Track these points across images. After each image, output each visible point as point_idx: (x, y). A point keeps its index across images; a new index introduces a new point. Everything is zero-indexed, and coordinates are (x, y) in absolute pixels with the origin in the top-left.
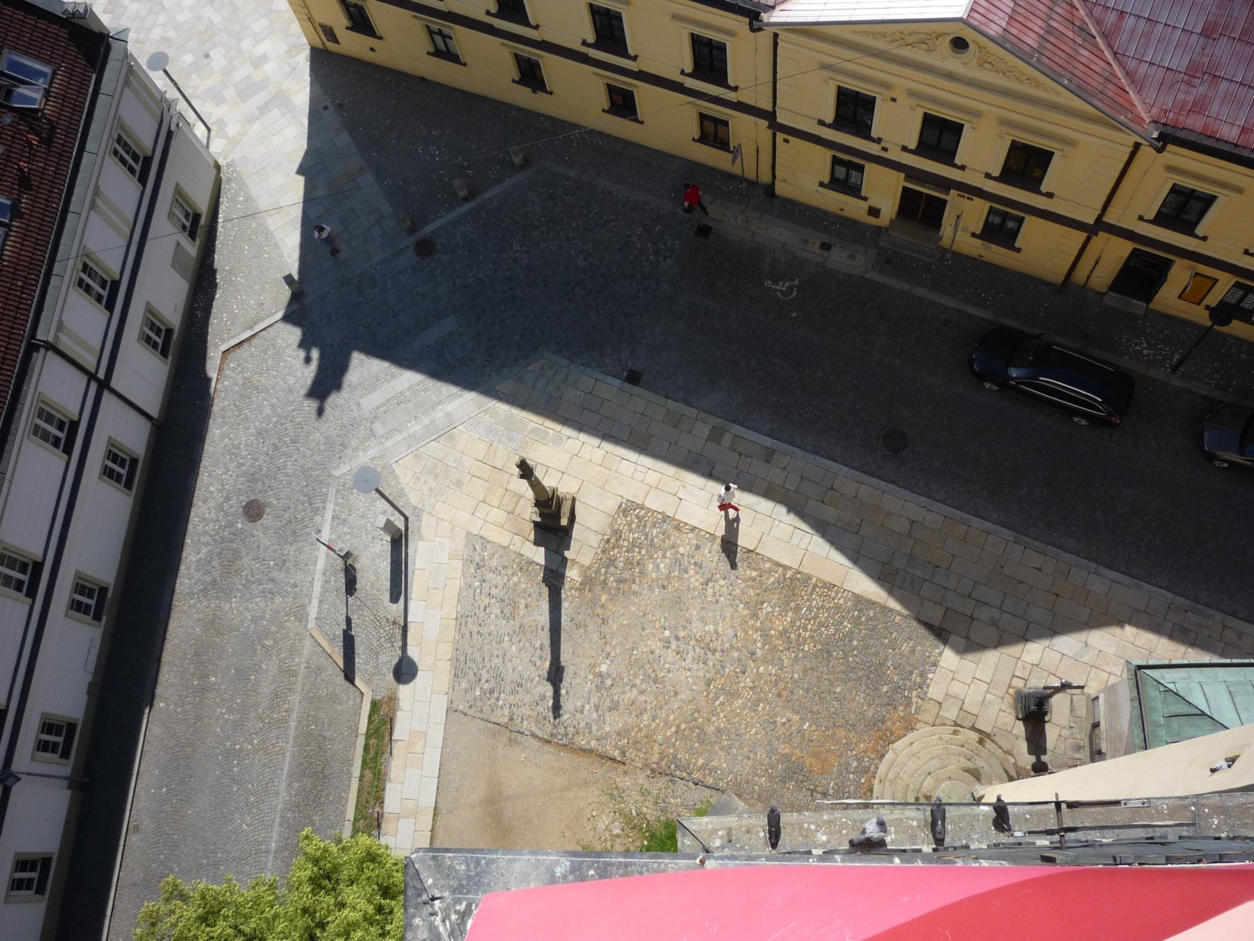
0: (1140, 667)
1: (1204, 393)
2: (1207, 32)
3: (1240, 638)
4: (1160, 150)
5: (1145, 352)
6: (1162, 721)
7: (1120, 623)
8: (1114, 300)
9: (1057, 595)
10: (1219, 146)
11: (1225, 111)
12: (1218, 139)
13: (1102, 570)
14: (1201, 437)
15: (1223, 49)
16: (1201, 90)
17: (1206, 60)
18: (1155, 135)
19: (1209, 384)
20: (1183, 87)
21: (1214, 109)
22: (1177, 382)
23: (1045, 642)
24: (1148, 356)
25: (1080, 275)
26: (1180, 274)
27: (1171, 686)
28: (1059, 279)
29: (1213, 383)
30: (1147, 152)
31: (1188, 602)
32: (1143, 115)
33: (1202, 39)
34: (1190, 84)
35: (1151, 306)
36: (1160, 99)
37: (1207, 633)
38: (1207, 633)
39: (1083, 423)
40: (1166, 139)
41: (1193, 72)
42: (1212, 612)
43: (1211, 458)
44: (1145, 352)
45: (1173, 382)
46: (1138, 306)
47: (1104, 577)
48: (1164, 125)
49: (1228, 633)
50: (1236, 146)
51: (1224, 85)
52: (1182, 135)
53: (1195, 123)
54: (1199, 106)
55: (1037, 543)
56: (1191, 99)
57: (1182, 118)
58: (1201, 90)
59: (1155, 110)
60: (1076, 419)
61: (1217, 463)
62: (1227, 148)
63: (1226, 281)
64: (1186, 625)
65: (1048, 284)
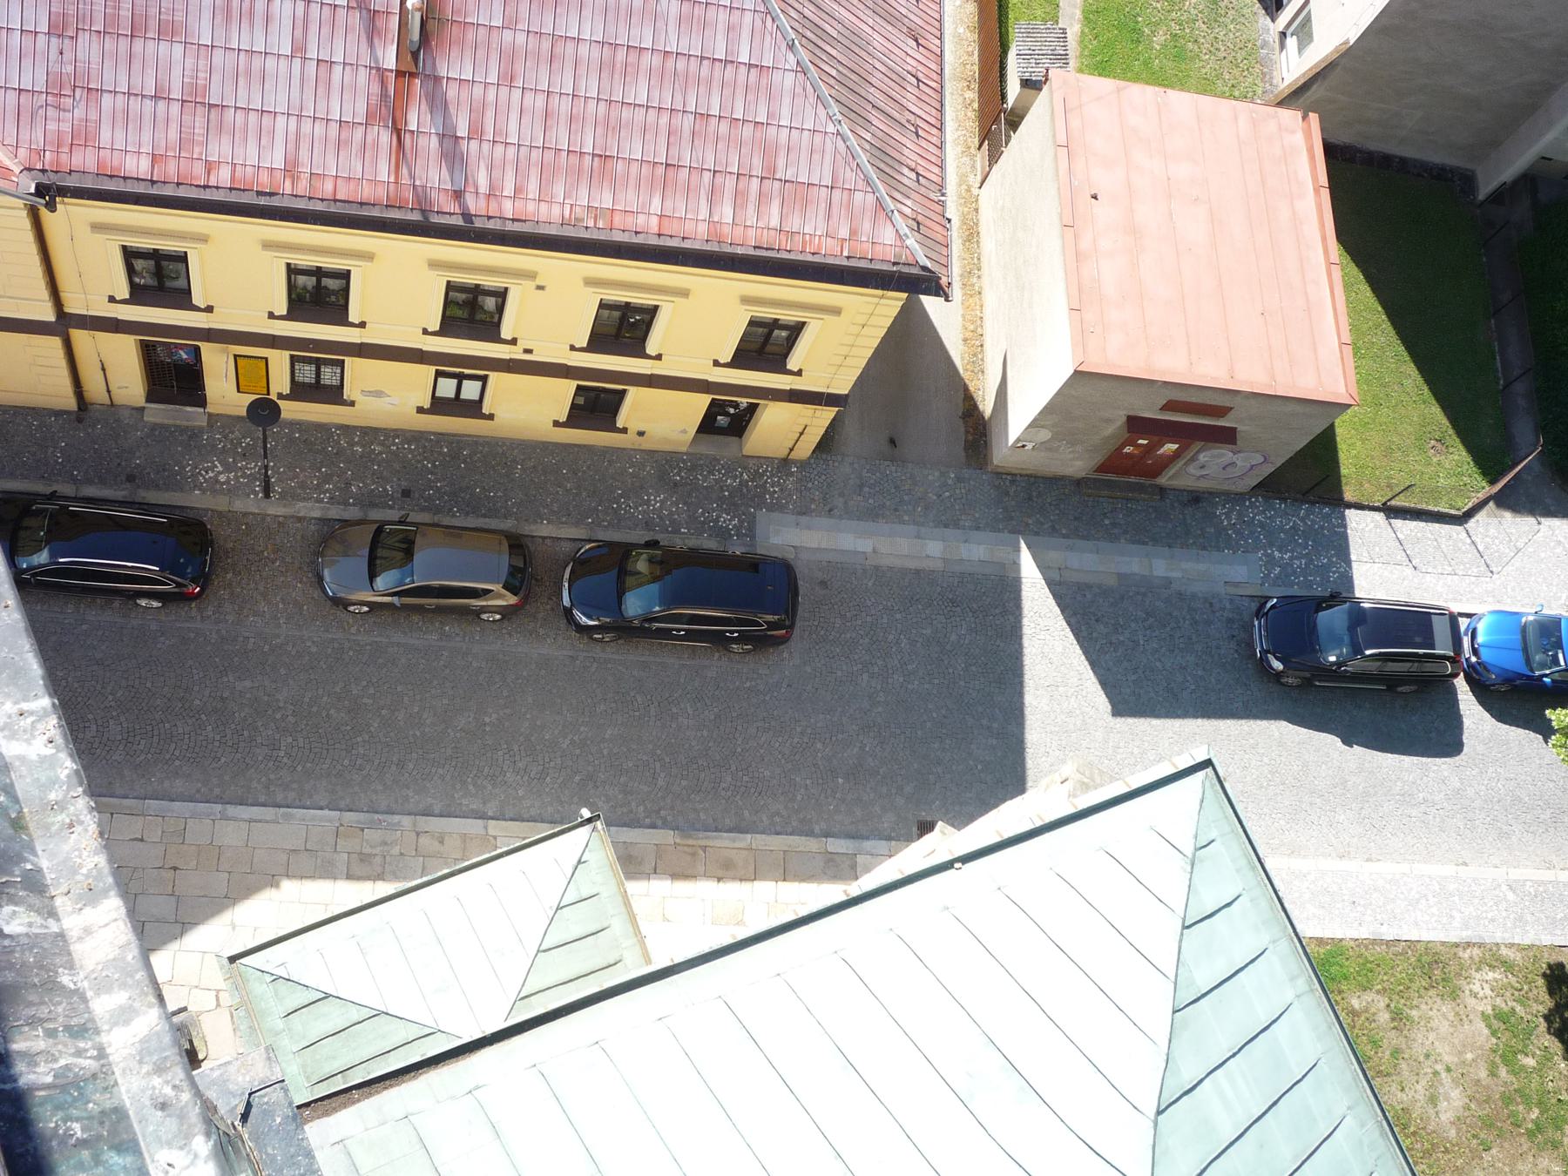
0: (232, 959)
1: (317, 514)
2: (57, 29)
3: (442, 842)
4: (51, 207)
5: (222, 478)
6: (280, 1024)
7: (273, 882)
8: (158, 413)
9: (175, 869)
10: (130, 188)
11: (120, 135)
12: (125, 178)
13: (232, 810)
14: (320, 579)
15: (88, 48)
16: (79, 113)
17: (69, 69)
18: (32, 190)
19: (321, 501)
20: (51, 112)
21: (106, 135)
22: (275, 509)
23: (174, 946)
24: (228, 482)
25: (94, 388)
26: (217, 364)
27: (281, 972)
28: (71, 403)
29: (326, 497)
30: (44, 212)
31: (362, 816)
32: (8, 163)
33: (54, 40)
34: (58, 107)
35: (210, 409)
36: (24, 135)
37: (396, 850)
38: (396, 850)
39: (155, 604)
40: (49, 193)
41: (59, 89)
42: (396, 818)
43: (341, 603)
44: (222, 478)
45: (272, 511)
46: (192, 415)
47: (235, 819)
48: (43, 171)
49: (423, 840)
50: (153, 182)
51: (107, 100)
52: (72, 182)
53: (84, 160)
54: (83, 136)
55: (126, 802)
56: (66, 127)
57: (64, 158)
58: (79, 113)
59: (22, 152)
60: (143, 602)
61: (351, 608)
62: (141, 189)
63: (279, 361)
64: (367, 850)
65: (58, 413)
